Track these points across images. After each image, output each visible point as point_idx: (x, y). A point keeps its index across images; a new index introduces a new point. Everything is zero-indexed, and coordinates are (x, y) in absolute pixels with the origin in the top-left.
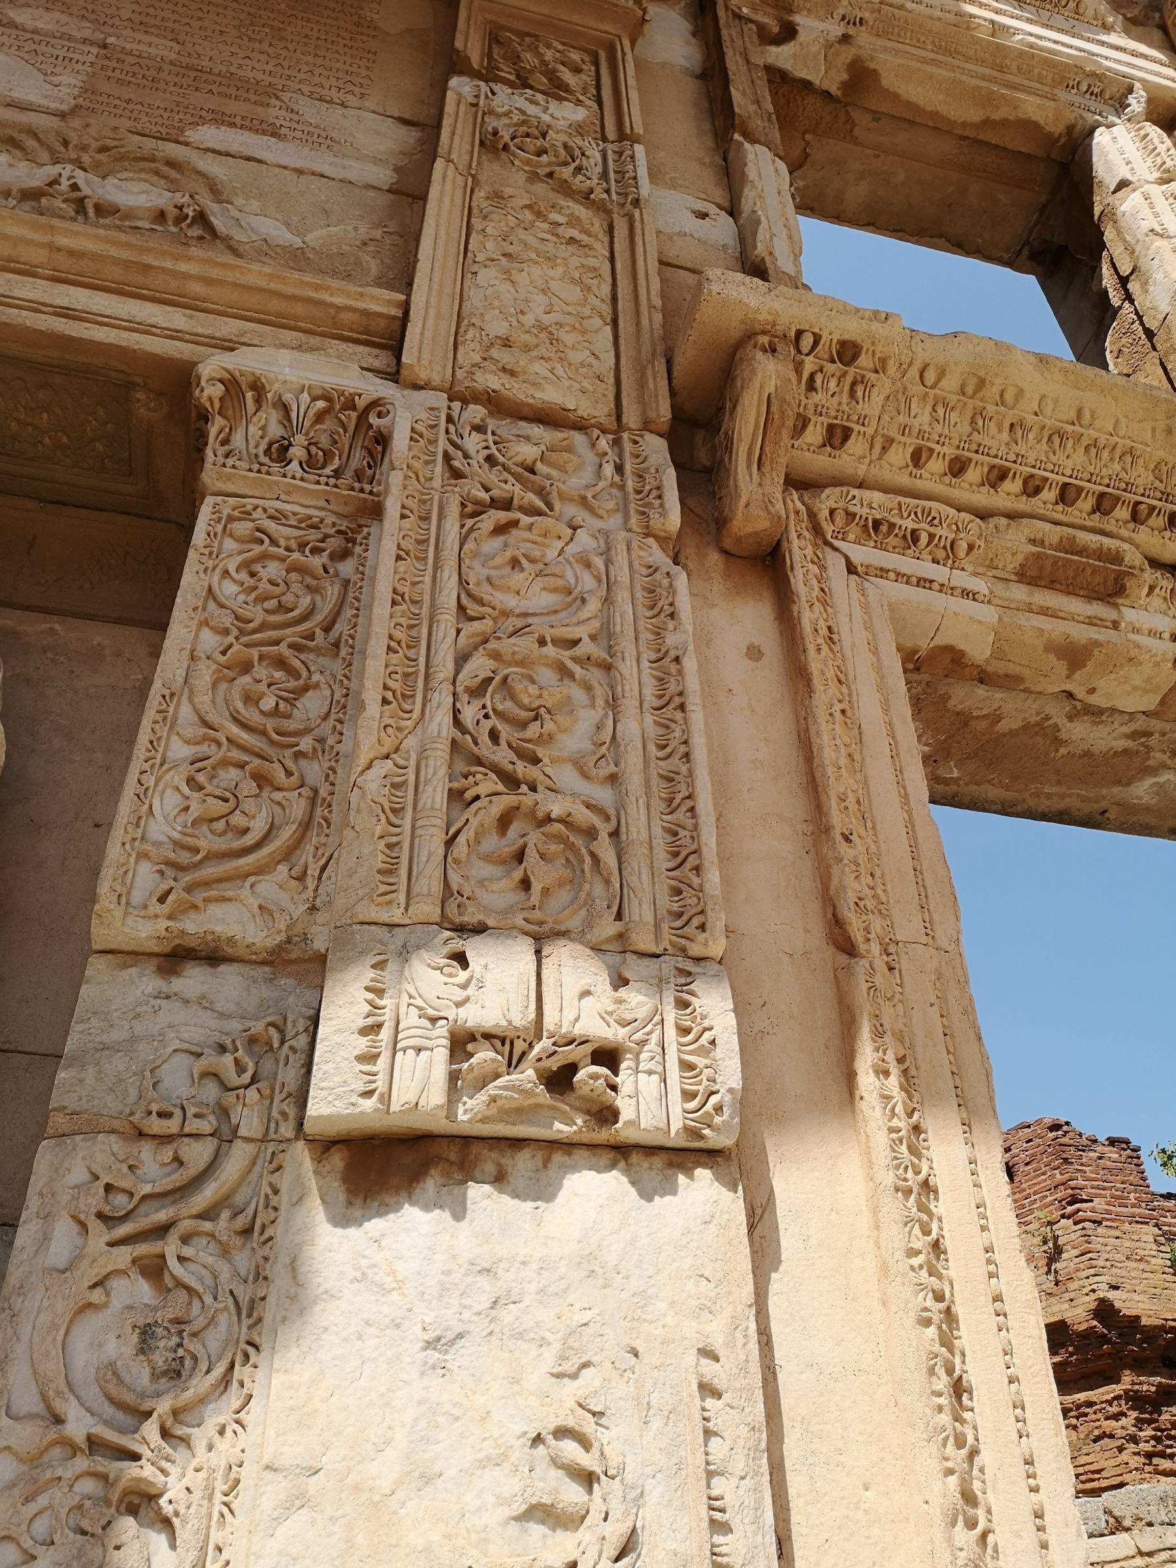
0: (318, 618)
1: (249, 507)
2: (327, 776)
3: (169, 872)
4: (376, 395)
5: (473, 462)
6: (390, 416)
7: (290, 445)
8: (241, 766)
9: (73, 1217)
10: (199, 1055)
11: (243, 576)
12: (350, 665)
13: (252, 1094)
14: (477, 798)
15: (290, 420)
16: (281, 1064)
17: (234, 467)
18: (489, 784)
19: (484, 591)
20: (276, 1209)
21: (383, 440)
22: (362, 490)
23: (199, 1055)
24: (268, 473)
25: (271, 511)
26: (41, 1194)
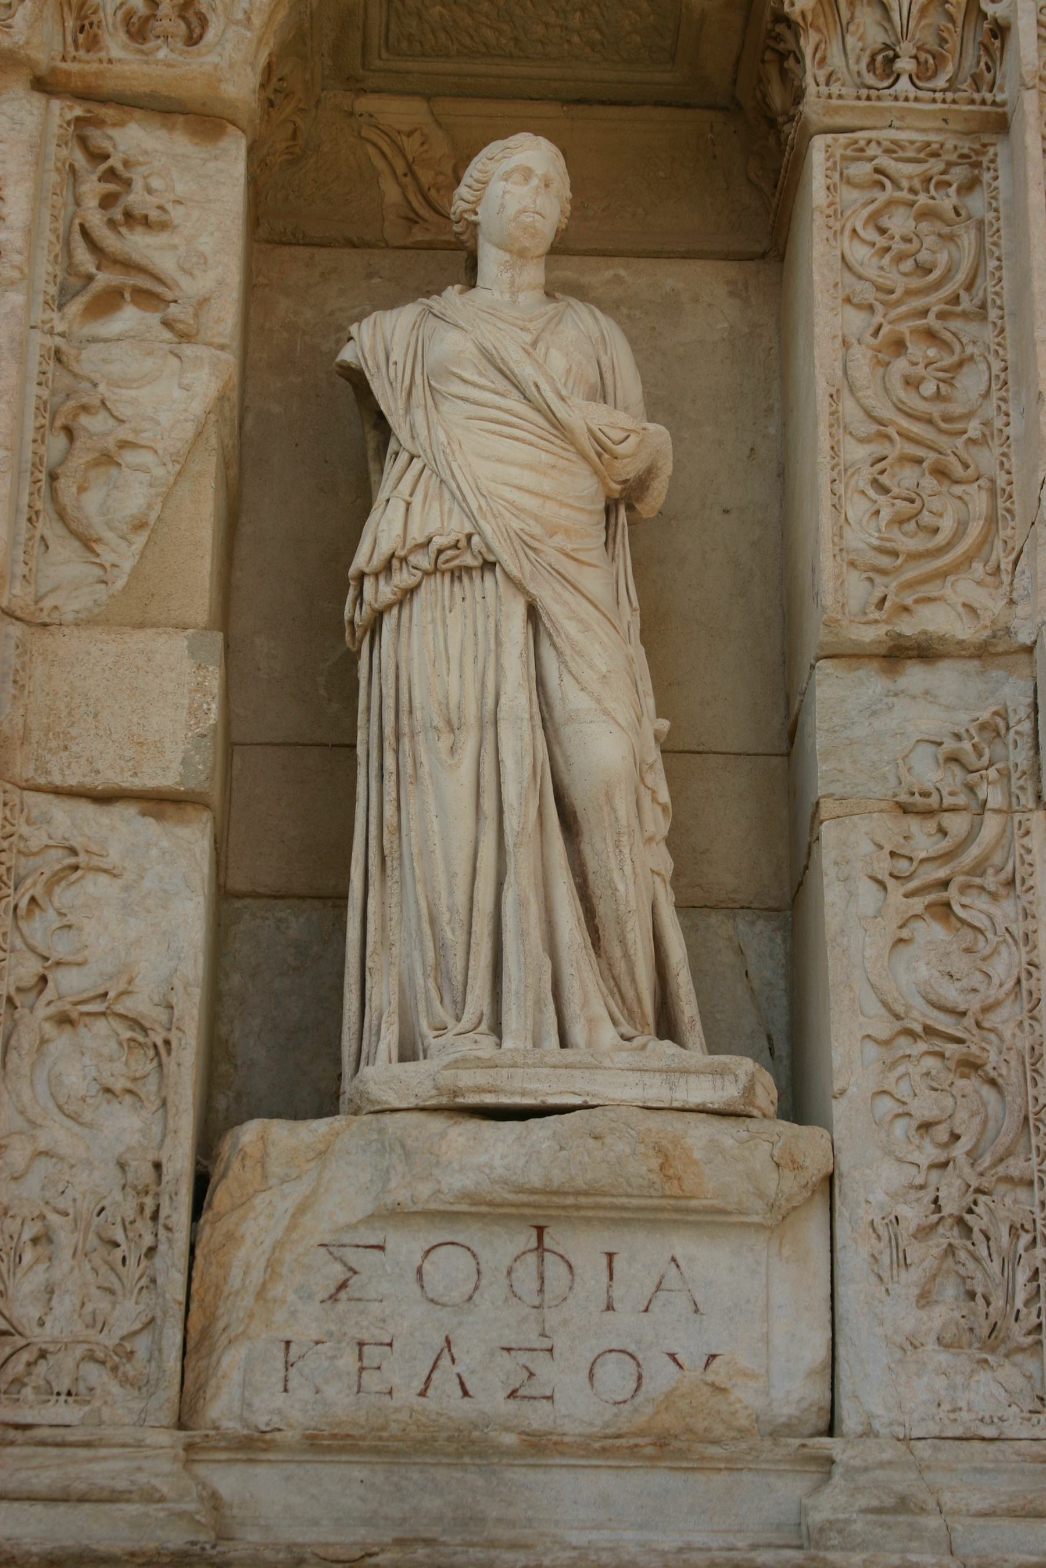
0: (961, 277)
1: (862, 143)
2: (1002, 463)
3: (878, 579)
10: (940, 744)
12: (1002, 331)
15: (889, 19)
16: (1011, 747)
17: (840, 97)
20: (1031, 865)
21: (1000, 31)
22: (983, 102)
23: (940, 744)
24: (879, 98)
25: (886, 144)
26: (836, 863)
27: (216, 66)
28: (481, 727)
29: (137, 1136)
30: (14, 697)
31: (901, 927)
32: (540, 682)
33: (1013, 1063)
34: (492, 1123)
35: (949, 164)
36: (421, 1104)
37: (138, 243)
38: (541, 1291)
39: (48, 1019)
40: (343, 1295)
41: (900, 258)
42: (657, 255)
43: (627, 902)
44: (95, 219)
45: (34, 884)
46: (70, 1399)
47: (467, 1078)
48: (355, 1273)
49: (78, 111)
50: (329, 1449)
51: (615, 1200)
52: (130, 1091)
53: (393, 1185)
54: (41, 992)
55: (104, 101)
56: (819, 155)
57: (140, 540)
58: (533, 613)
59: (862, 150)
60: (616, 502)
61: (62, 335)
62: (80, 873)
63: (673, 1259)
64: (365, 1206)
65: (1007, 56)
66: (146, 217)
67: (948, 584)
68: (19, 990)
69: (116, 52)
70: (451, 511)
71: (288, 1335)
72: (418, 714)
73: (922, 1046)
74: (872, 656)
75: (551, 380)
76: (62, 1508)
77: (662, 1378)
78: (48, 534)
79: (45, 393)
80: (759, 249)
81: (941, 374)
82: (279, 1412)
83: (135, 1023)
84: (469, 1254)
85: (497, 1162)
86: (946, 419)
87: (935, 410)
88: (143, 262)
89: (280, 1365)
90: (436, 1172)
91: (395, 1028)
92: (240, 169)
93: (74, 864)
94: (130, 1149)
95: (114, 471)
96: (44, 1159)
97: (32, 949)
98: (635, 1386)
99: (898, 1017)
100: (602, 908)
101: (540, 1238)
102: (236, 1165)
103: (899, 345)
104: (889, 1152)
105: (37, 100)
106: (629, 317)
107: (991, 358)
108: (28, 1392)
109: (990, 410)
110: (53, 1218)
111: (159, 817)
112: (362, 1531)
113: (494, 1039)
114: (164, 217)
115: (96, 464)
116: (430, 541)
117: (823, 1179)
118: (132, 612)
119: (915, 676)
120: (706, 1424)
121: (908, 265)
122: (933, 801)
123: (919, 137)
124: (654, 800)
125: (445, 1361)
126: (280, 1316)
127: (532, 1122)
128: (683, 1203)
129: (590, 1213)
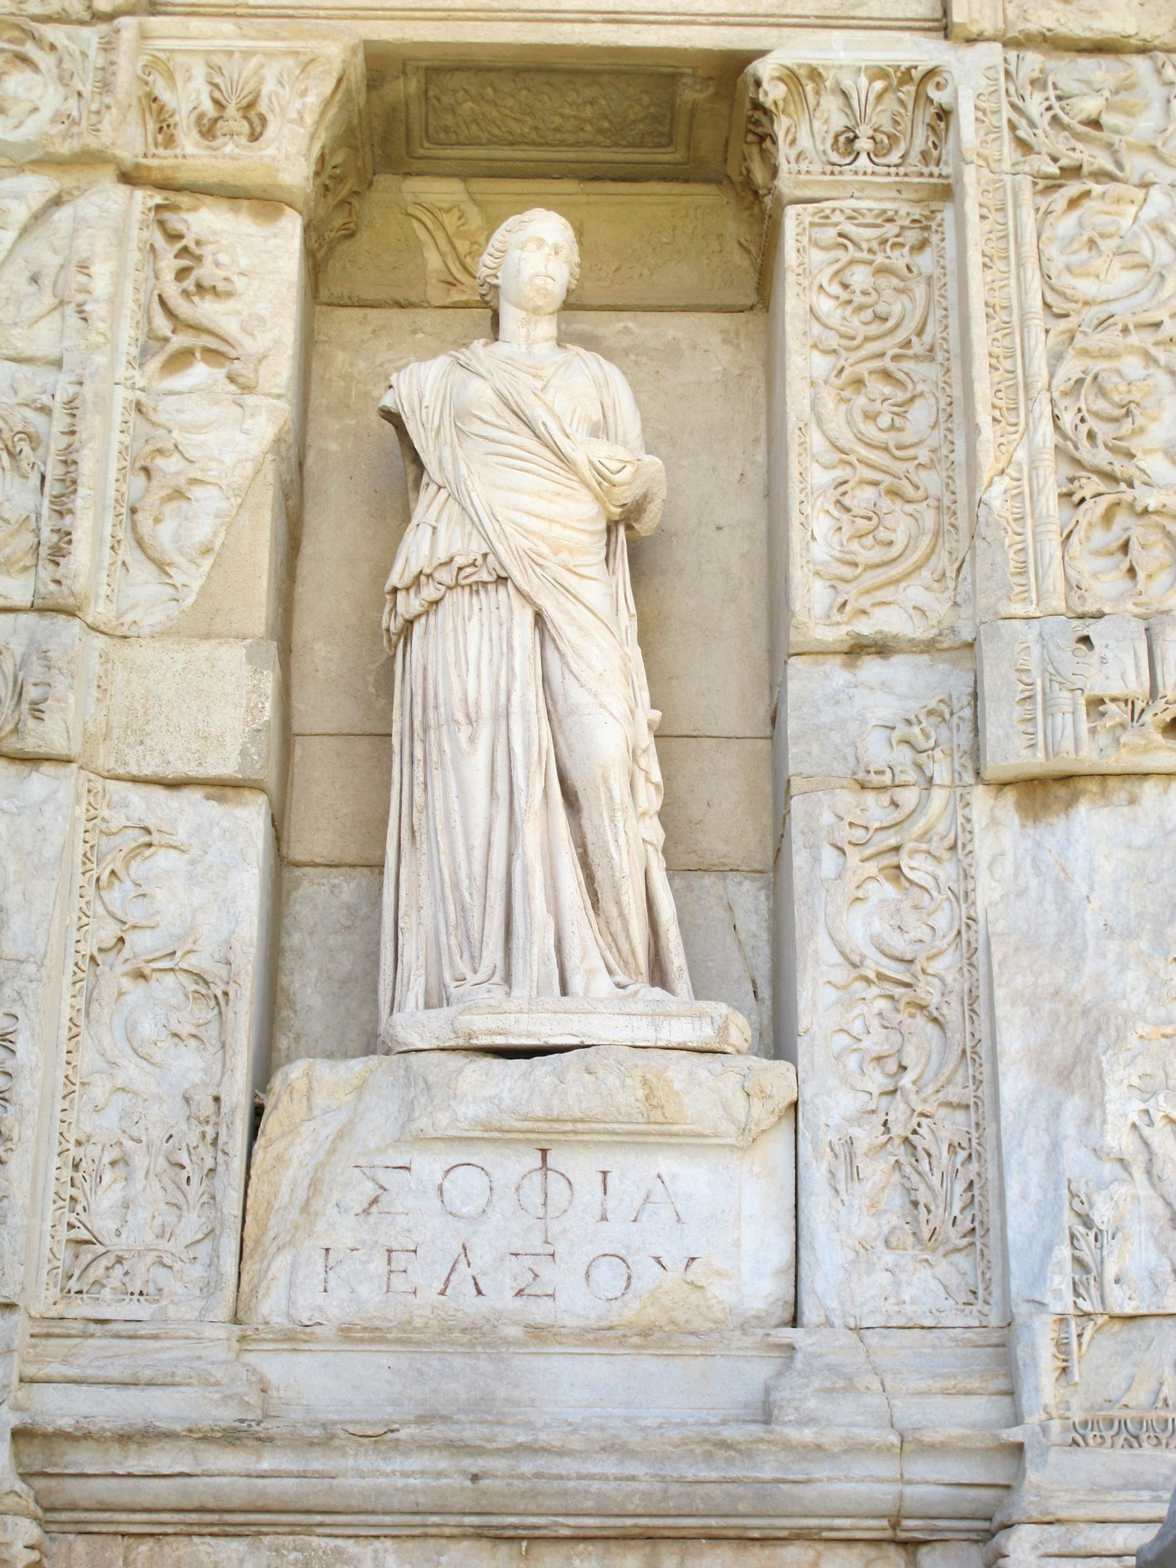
0: (911, 325)
1: (828, 212)
3: (842, 587)
4: (931, 65)
5: (1039, 132)
6: (950, 88)
7: (856, 137)
8: (876, 484)
10: (893, 728)
11: (835, 289)
12: (948, 370)
13: (938, 754)
14: (1083, 500)
15: (850, 106)
18: (1091, 485)
19: (1066, 281)
21: (944, 114)
22: (931, 175)
23: (893, 728)
24: (841, 173)
26: (803, 833)
27: (274, 158)
28: (495, 719)
29: (200, 1074)
30: (98, 699)
31: (858, 887)
32: (546, 680)
33: (953, 1004)
34: (502, 1061)
35: (902, 228)
36: (442, 1045)
37: (206, 310)
38: (545, 1204)
39: (126, 974)
40: (374, 1209)
41: (861, 308)
42: (661, 309)
44: (172, 291)
45: (114, 860)
46: (142, 1298)
49: (158, 199)
50: (362, 1341)
51: (607, 1126)
52: (194, 1036)
53: (417, 1114)
54: (119, 951)
55: (179, 189)
56: (793, 221)
57: (207, 563)
58: (539, 618)
59: (827, 217)
60: (617, 523)
61: (143, 390)
62: (153, 849)
63: (659, 1176)
65: (951, 136)
66: (214, 287)
67: (901, 589)
68: (100, 950)
69: (190, 149)
70: (470, 534)
72: (442, 710)
73: (875, 990)
75: (558, 420)
76: (132, 1392)
77: (647, 1276)
78: (128, 560)
79: (127, 439)
80: (748, 302)
81: (896, 409)
82: (320, 1309)
83: (199, 978)
85: (505, 1095)
86: (900, 448)
87: (890, 438)
88: (211, 326)
89: (320, 1268)
90: (452, 1103)
91: (422, 980)
92: (295, 244)
93: (148, 840)
94: (195, 1086)
95: (184, 505)
96: (121, 1095)
97: (112, 915)
98: (624, 1285)
99: (855, 966)
100: (600, 874)
101: (544, 1159)
102: (285, 1098)
103: (859, 382)
104: (845, 1080)
105: (123, 189)
106: (636, 362)
107: (939, 394)
108: (106, 1293)
109: (935, 439)
110: (129, 1144)
111: (221, 799)
112: (389, 1409)
113: (506, 988)
114: (229, 288)
115: (170, 498)
116: (451, 560)
117: (790, 1106)
118: (200, 626)
119: (871, 668)
121: (868, 314)
122: (887, 779)
123: (877, 206)
124: (648, 780)
125: (462, 1265)
126: (321, 1226)
127: (536, 1060)
128: (666, 1128)
129: (586, 1138)
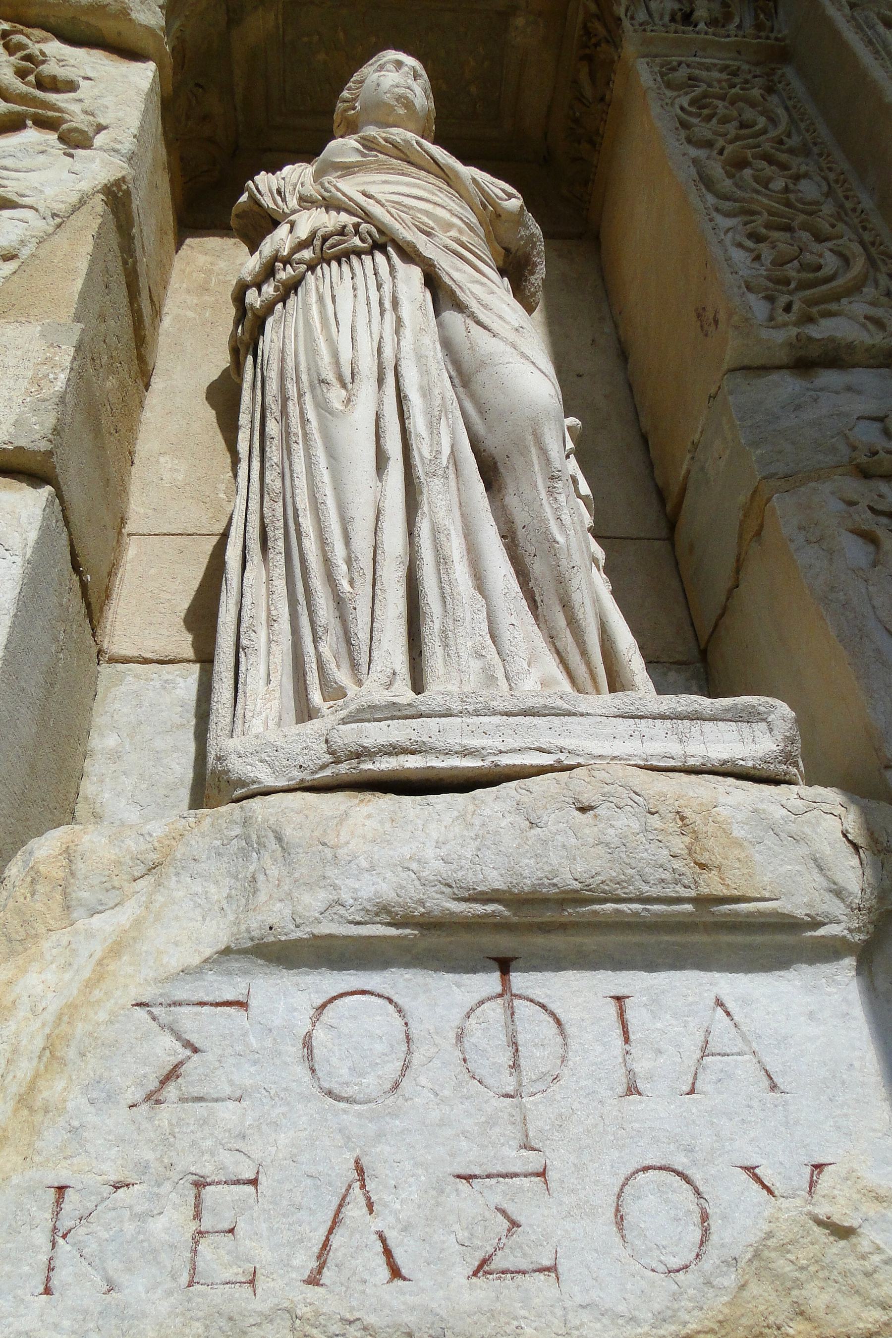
1: (675, 64)
9: (852, 532)
38: (515, 1066)
40: (171, 1091)
43: (570, 555)
47: (376, 734)
48: (195, 1050)
53: (262, 897)
63: (719, 1003)
64: (216, 933)
71: (63, 1176)
74: (779, 368)
84: (391, 1008)
85: (430, 853)
89: (41, 1238)
90: (331, 872)
98: (698, 1235)
120: (825, 1298)
125: (355, 1211)
126: (52, 1137)
